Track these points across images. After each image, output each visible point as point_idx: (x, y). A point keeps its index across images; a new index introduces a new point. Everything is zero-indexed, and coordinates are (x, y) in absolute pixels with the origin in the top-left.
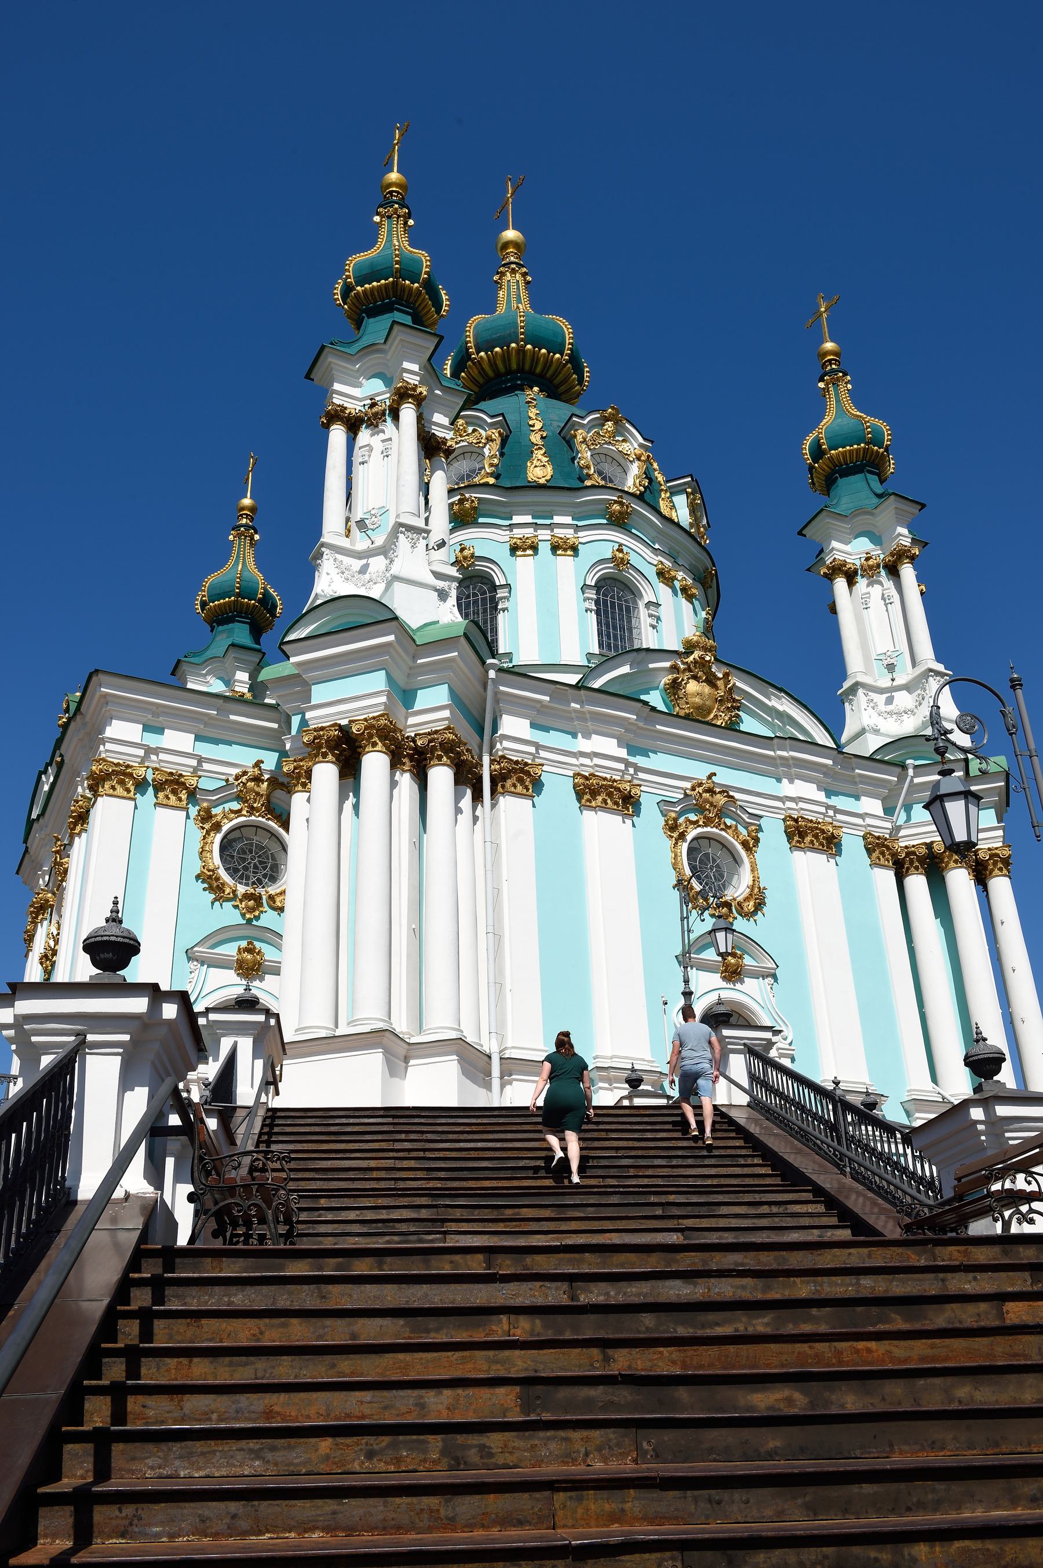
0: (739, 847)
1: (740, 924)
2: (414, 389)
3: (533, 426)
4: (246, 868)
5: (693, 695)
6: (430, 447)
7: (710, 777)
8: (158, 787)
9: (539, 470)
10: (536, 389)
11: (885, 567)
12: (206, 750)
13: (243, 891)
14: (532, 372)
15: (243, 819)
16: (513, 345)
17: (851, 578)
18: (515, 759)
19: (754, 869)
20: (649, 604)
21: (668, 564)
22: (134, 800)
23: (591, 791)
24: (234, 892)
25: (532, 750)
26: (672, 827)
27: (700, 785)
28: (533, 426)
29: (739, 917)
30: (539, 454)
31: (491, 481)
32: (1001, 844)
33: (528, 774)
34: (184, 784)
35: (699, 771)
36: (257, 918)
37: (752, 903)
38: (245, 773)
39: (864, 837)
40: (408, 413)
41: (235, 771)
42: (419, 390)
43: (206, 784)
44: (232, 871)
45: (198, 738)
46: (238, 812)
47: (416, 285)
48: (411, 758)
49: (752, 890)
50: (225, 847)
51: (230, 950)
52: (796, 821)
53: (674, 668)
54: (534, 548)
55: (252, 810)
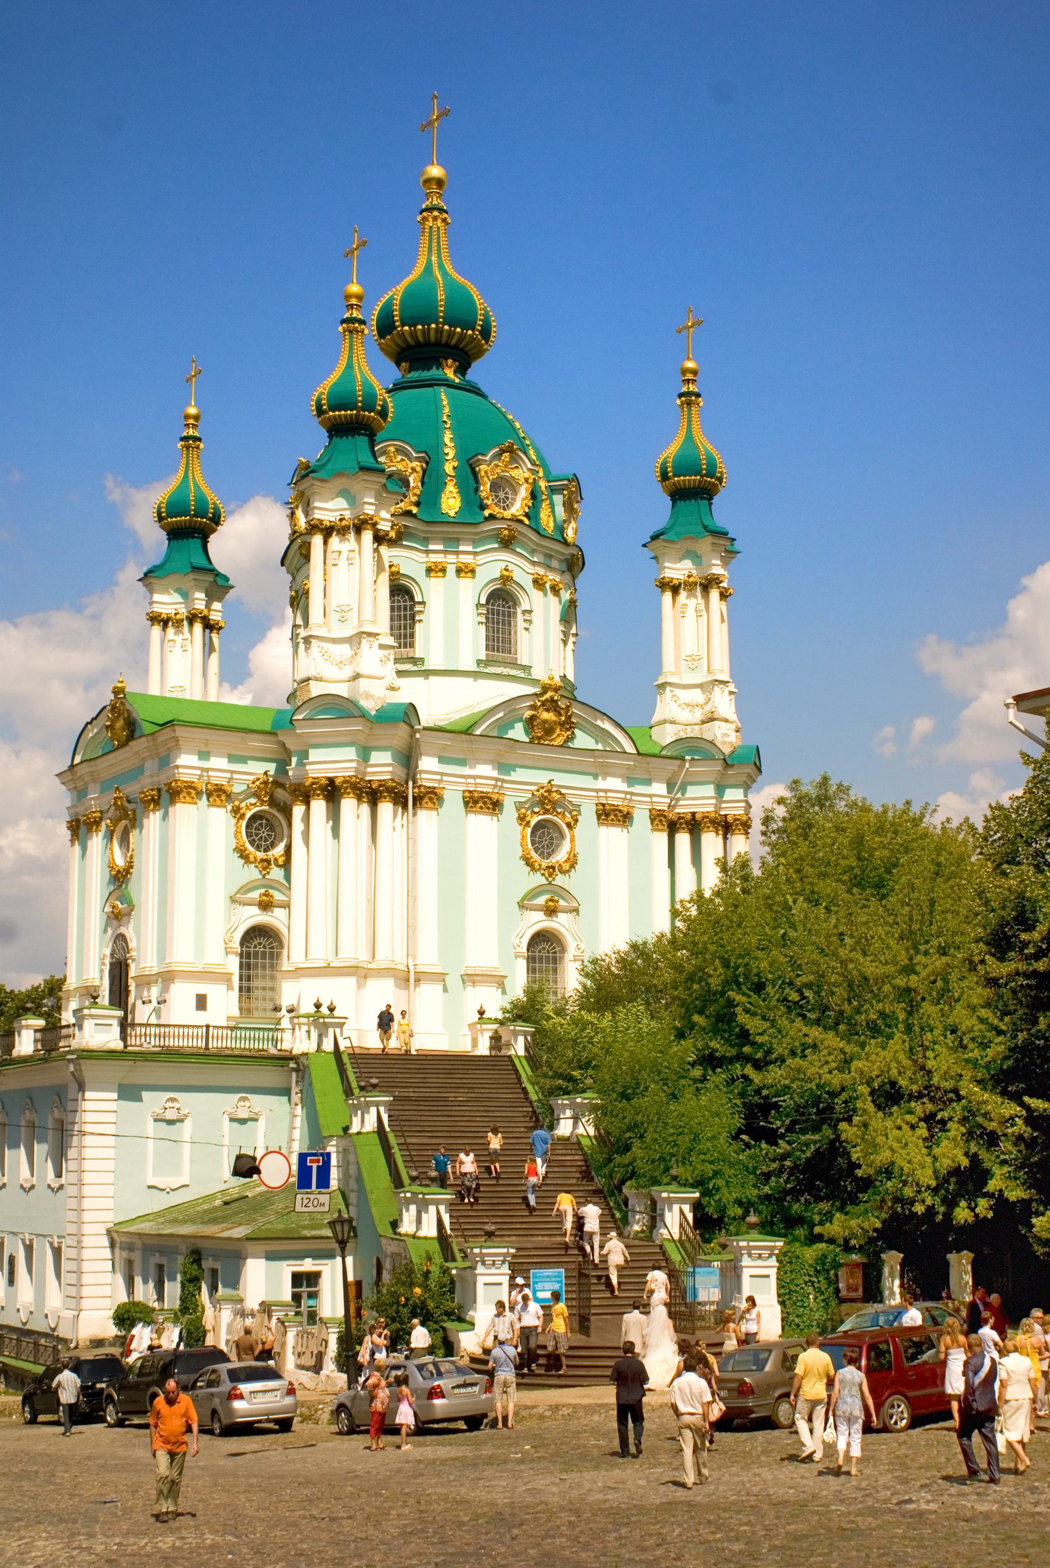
0: (564, 826)
1: (560, 880)
2: (371, 519)
3: (447, 454)
6: (379, 538)
8: (209, 795)
9: (451, 502)
10: (450, 361)
11: (701, 584)
14: (447, 345)
17: (675, 590)
18: (428, 785)
19: (572, 840)
20: (524, 612)
21: (541, 571)
25: (439, 777)
26: (521, 819)
28: (447, 454)
30: (451, 487)
31: (415, 510)
32: (742, 812)
33: (436, 794)
35: (542, 777)
36: (268, 873)
37: (566, 867)
38: (258, 779)
39: (650, 810)
40: (368, 536)
43: (237, 788)
44: (252, 843)
48: (367, 793)
50: (247, 827)
51: (255, 895)
52: (604, 805)
53: (533, 707)
54: (443, 570)
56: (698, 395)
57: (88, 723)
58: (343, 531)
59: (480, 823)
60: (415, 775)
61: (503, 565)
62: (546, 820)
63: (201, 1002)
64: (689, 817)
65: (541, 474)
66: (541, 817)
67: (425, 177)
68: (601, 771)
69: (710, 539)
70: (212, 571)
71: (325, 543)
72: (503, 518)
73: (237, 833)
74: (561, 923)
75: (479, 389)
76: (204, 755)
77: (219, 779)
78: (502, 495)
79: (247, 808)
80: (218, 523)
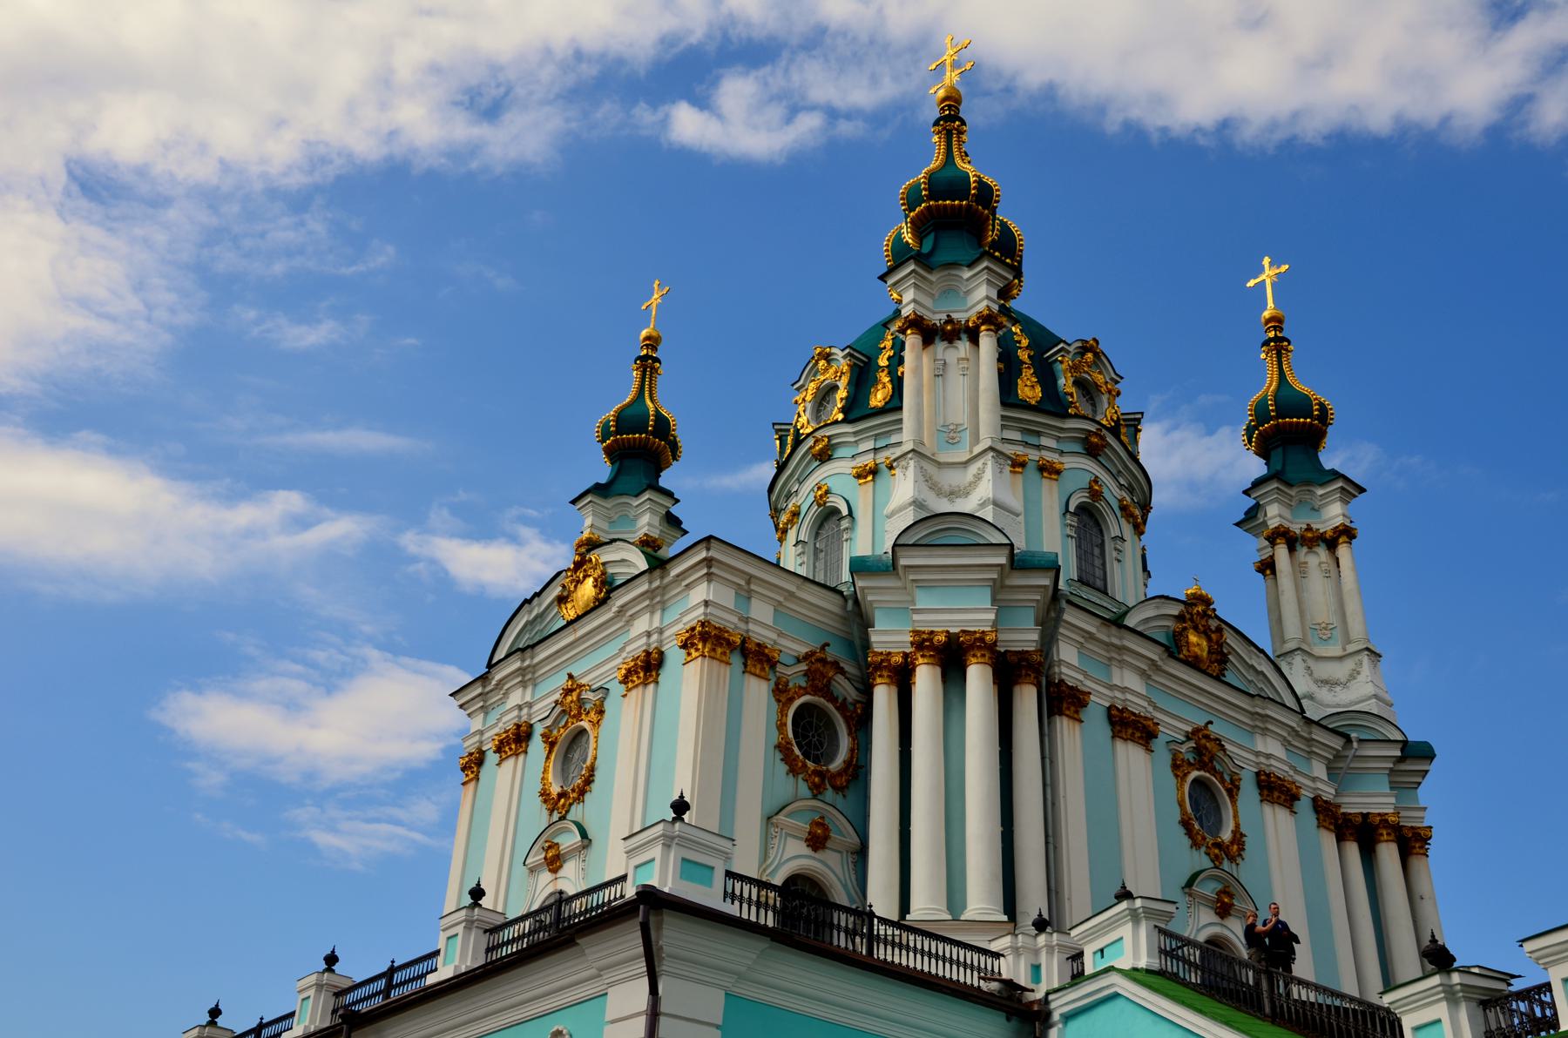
1: (1226, 865)
19: (1236, 816)
25: (1081, 677)
38: (813, 653)
40: (987, 342)
41: (804, 650)
43: (783, 659)
52: (1268, 775)
53: (1180, 618)
55: (815, 690)
57: (527, 602)
64: (1360, 819)
66: (1195, 774)
68: (1261, 724)
69: (1340, 484)
70: (668, 494)
73: (781, 726)
77: (762, 634)
80: (675, 458)
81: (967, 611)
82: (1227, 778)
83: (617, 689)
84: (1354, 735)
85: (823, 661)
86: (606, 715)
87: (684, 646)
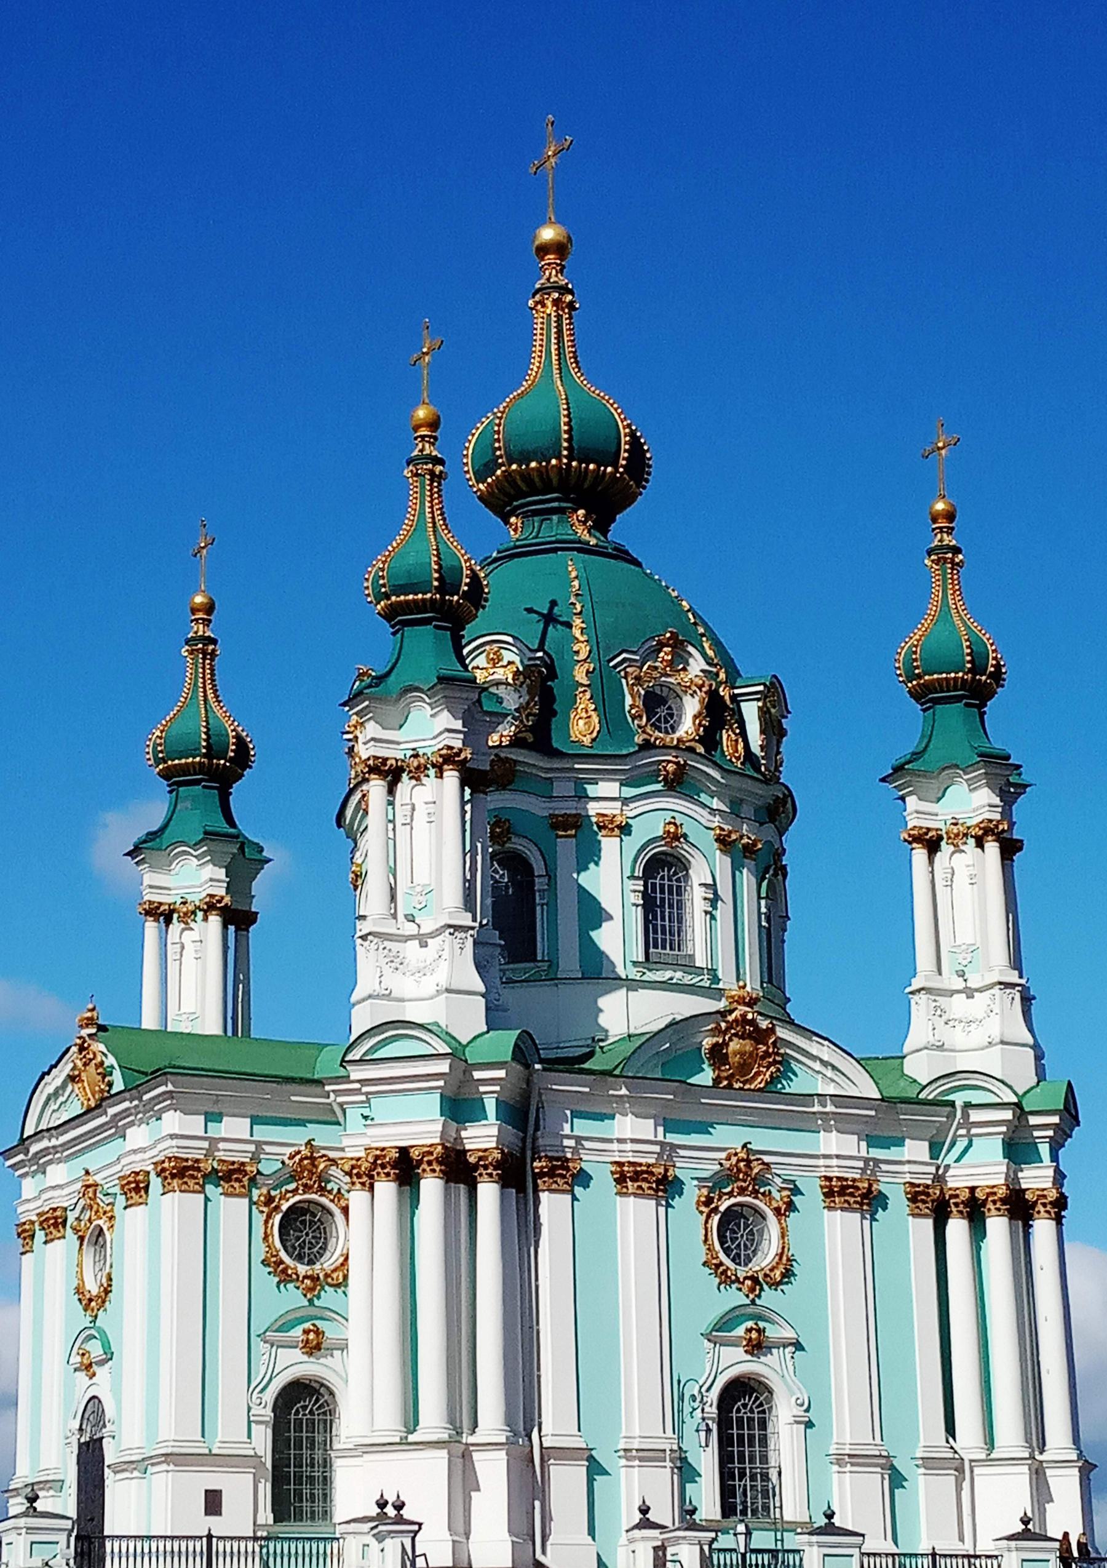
3: (577, 652)
4: (302, 1247)
5: (735, 1054)
7: (745, 1146)
10: (581, 512)
12: (263, 1133)
13: (304, 1273)
15: (297, 1198)
16: (554, 462)
17: (933, 846)
19: (783, 1235)
22: (203, 1191)
23: (627, 1177)
24: (296, 1274)
27: (736, 1154)
28: (577, 652)
29: (765, 1287)
30: (584, 701)
34: (245, 1171)
37: (777, 1274)
38: (299, 1152)
42: (463, 756)
45: (255, 1120)
46: (295, 1191)
47: (456, 598)
49: (781, 1259)
51: (297, 1332)
52: (829, 1179)
56: (956, 550)
58: (418, 773)
59: (636, 1213)
60: (535, 1139)
61: (668, 816)
62: (740, 1205)
63: (213, 1503)
64: (965, 1195)
65: (722, 676)
66: (733, 1201)
67: (537, 243)
71: (391, 791)
72: (665, 747)
73: (266, 1238)
74: (768, 1367)
75: (627, 552)
76: (213, 1117)
78: (662, 712)
79: (283, 1197)
81: (417, 1123)
82: (776, 1195)
83: (121, 1201)
84: (959, 1098)
85: (312, 1158)
86: (117, 1223)
87: (158, 1175)
